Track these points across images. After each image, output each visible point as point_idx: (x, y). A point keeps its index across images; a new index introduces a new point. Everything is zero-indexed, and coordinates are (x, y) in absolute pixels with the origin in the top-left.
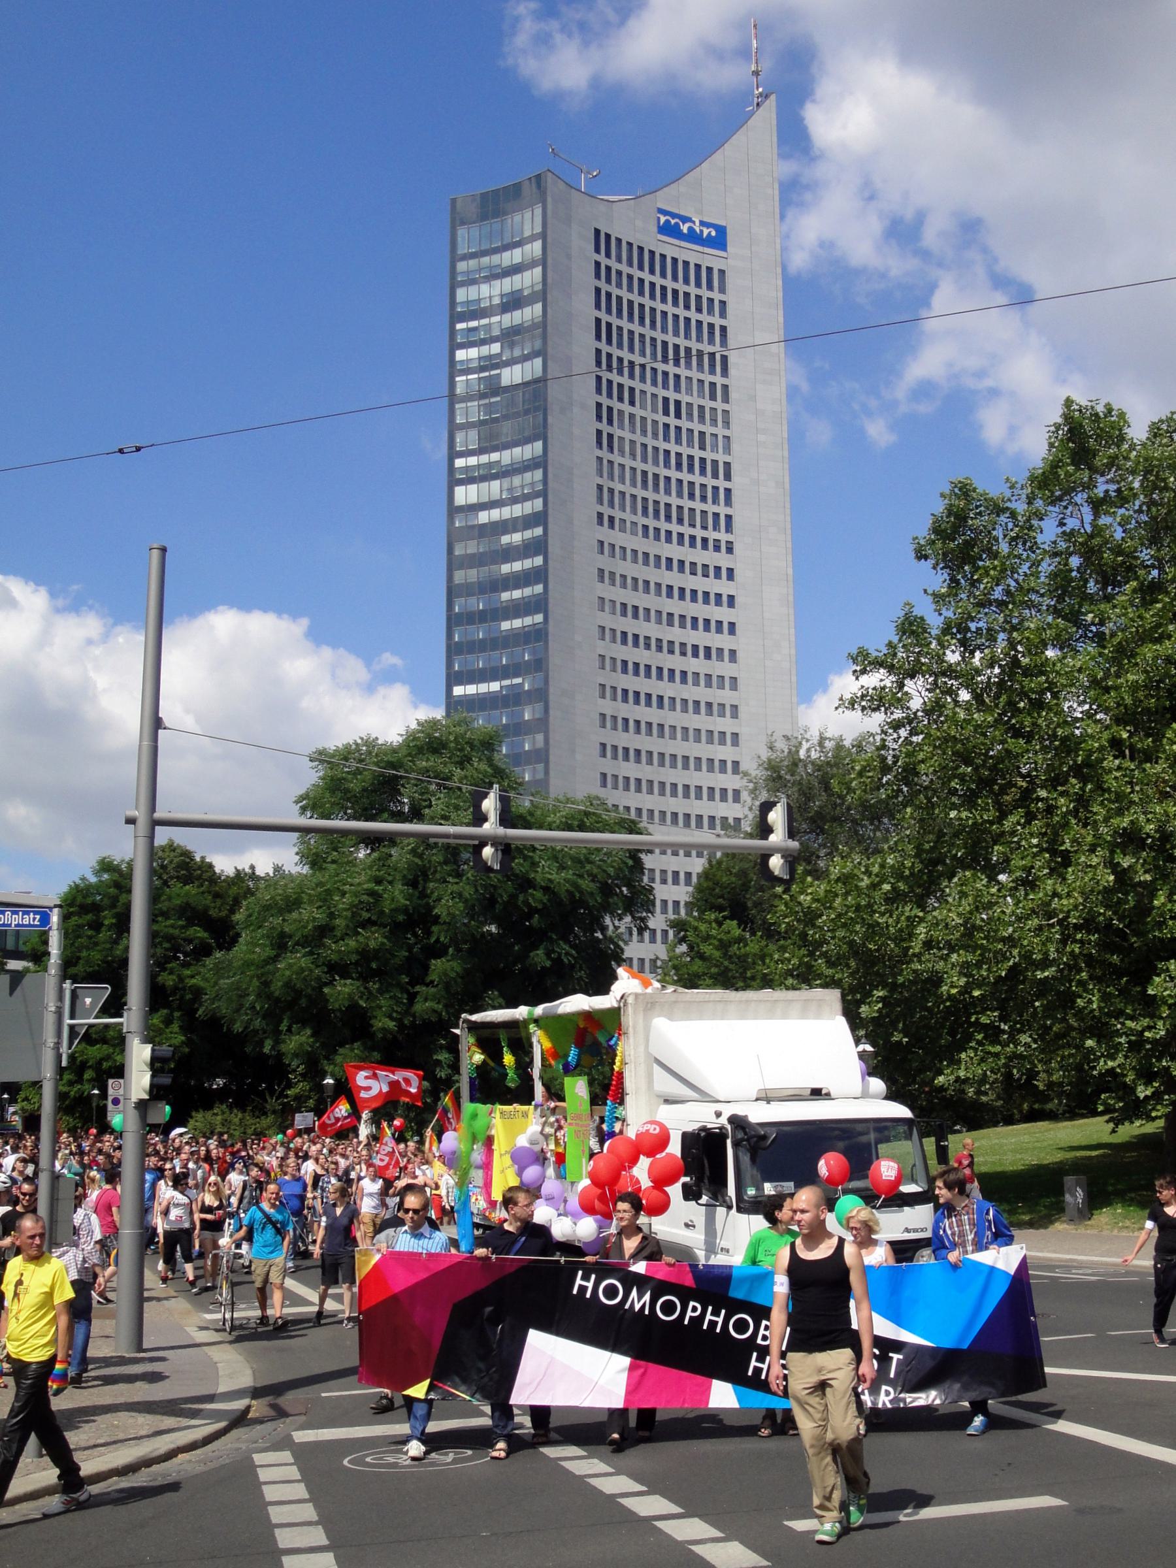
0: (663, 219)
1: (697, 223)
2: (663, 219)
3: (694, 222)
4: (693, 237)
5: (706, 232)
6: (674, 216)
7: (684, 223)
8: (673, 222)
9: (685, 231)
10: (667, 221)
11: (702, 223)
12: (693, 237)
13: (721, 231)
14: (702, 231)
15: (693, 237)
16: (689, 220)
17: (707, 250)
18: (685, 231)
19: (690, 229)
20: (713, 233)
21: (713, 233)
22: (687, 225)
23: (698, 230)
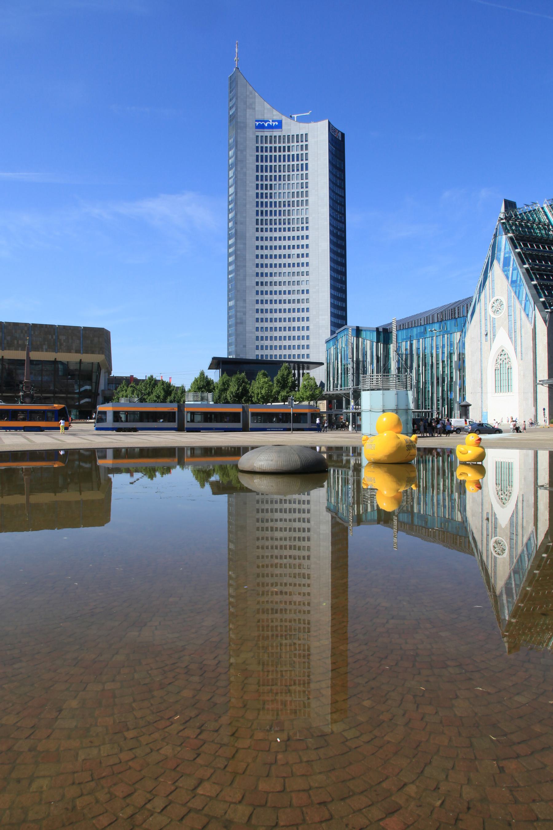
0: (257, 123)
1: (271, 121)
2: (257, 123)
6: (261, 121)
9: (266, 125)
11: (273, 121)
12: (270, 127)
13: (280, 122)
15: (270, 127)
16: (268, 121)
17: (274, 130)
18: (266, 125)
19: (269, 124)
20: (277, 124)
21: (277, 124)
22: (267, 123)
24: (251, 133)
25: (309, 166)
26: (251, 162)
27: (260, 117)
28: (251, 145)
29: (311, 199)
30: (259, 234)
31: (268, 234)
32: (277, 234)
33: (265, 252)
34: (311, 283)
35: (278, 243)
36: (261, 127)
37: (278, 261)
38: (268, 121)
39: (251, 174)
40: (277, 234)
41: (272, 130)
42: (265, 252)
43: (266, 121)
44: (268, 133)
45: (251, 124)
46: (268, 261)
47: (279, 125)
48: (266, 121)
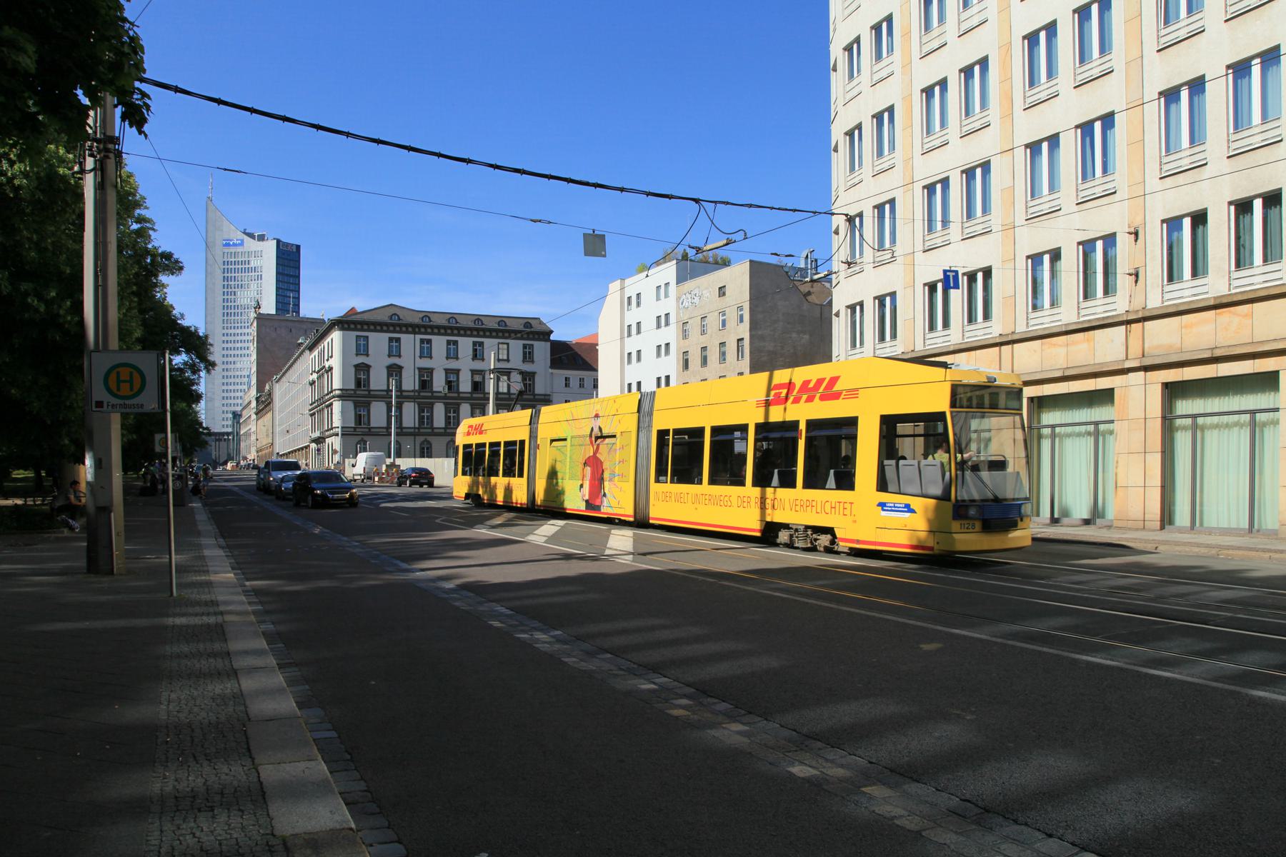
4: (235, 245)
24: (219, 250)
26: (219, 275)
27: (226, 237)
28: (220, 261)
30: (225, 331)
31: (232, 331)
32: (239, 331)
33: (230, 345)
35: (239, 338)
36: (227, 245)
37: (239, 352)
39: (219, 282)
40: (239, 331)
42: (230, 345)
44: (232, 250)
45: (220, 242)
46: (232, 352)
47: (242, 244)
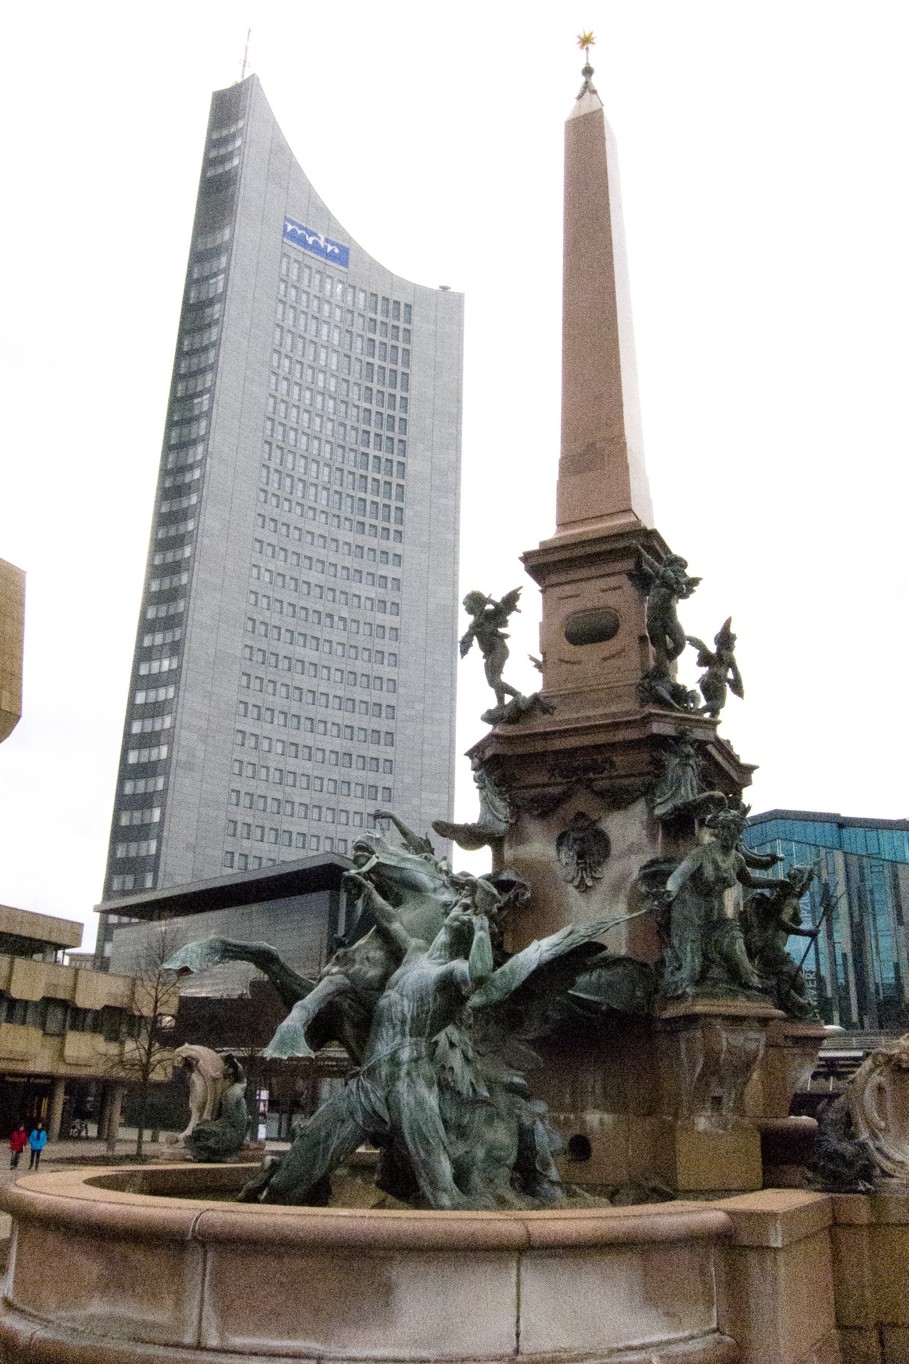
1: (323, 239)
2: (290, 227)
3: (319, 238)
5: (330, 248)
7: (310, 236)
8: (299, 232)
10: (293, 230)
11: (327, 240)
13: (345, 251)
14: (326, 247)
16: (316, 235)
18: (310, 240)
19: (315, 242)
20: (337, 251)
21: (337, 251)
23: (322, 243)
25: (413, 381)
29: (414, 465)
34: (401, 690)
38: (316, 235)
41: (324, 260)
43: (312, 234)
48: (312, 234)
